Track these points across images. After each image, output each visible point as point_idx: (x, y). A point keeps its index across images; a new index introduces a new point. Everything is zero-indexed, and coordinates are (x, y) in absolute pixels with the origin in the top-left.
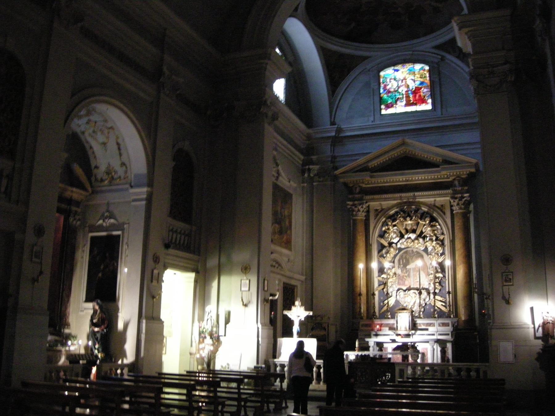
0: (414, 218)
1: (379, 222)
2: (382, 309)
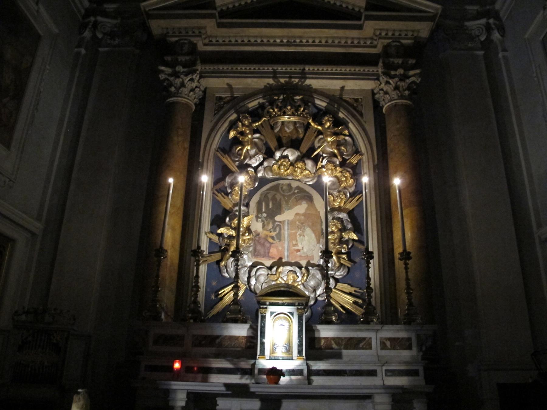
0: (302, 109)
1: (222, 121)
2: (212, 308)
